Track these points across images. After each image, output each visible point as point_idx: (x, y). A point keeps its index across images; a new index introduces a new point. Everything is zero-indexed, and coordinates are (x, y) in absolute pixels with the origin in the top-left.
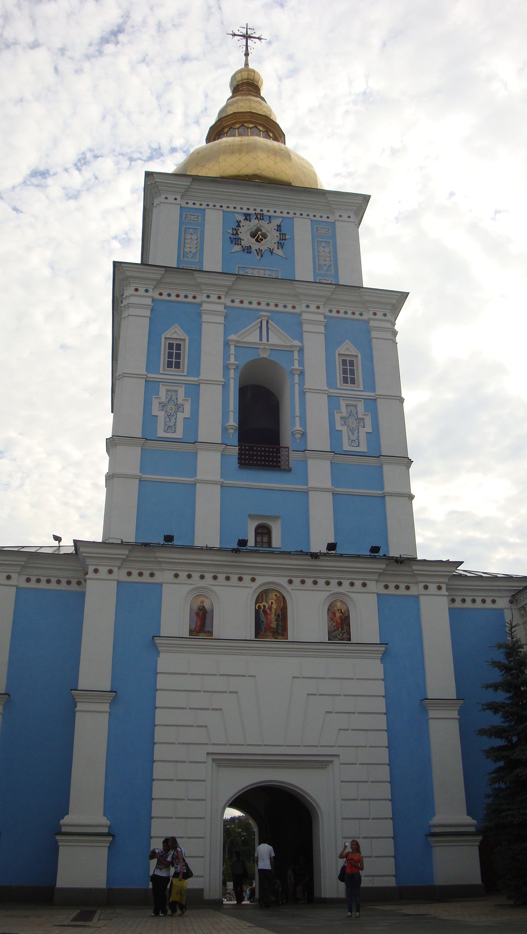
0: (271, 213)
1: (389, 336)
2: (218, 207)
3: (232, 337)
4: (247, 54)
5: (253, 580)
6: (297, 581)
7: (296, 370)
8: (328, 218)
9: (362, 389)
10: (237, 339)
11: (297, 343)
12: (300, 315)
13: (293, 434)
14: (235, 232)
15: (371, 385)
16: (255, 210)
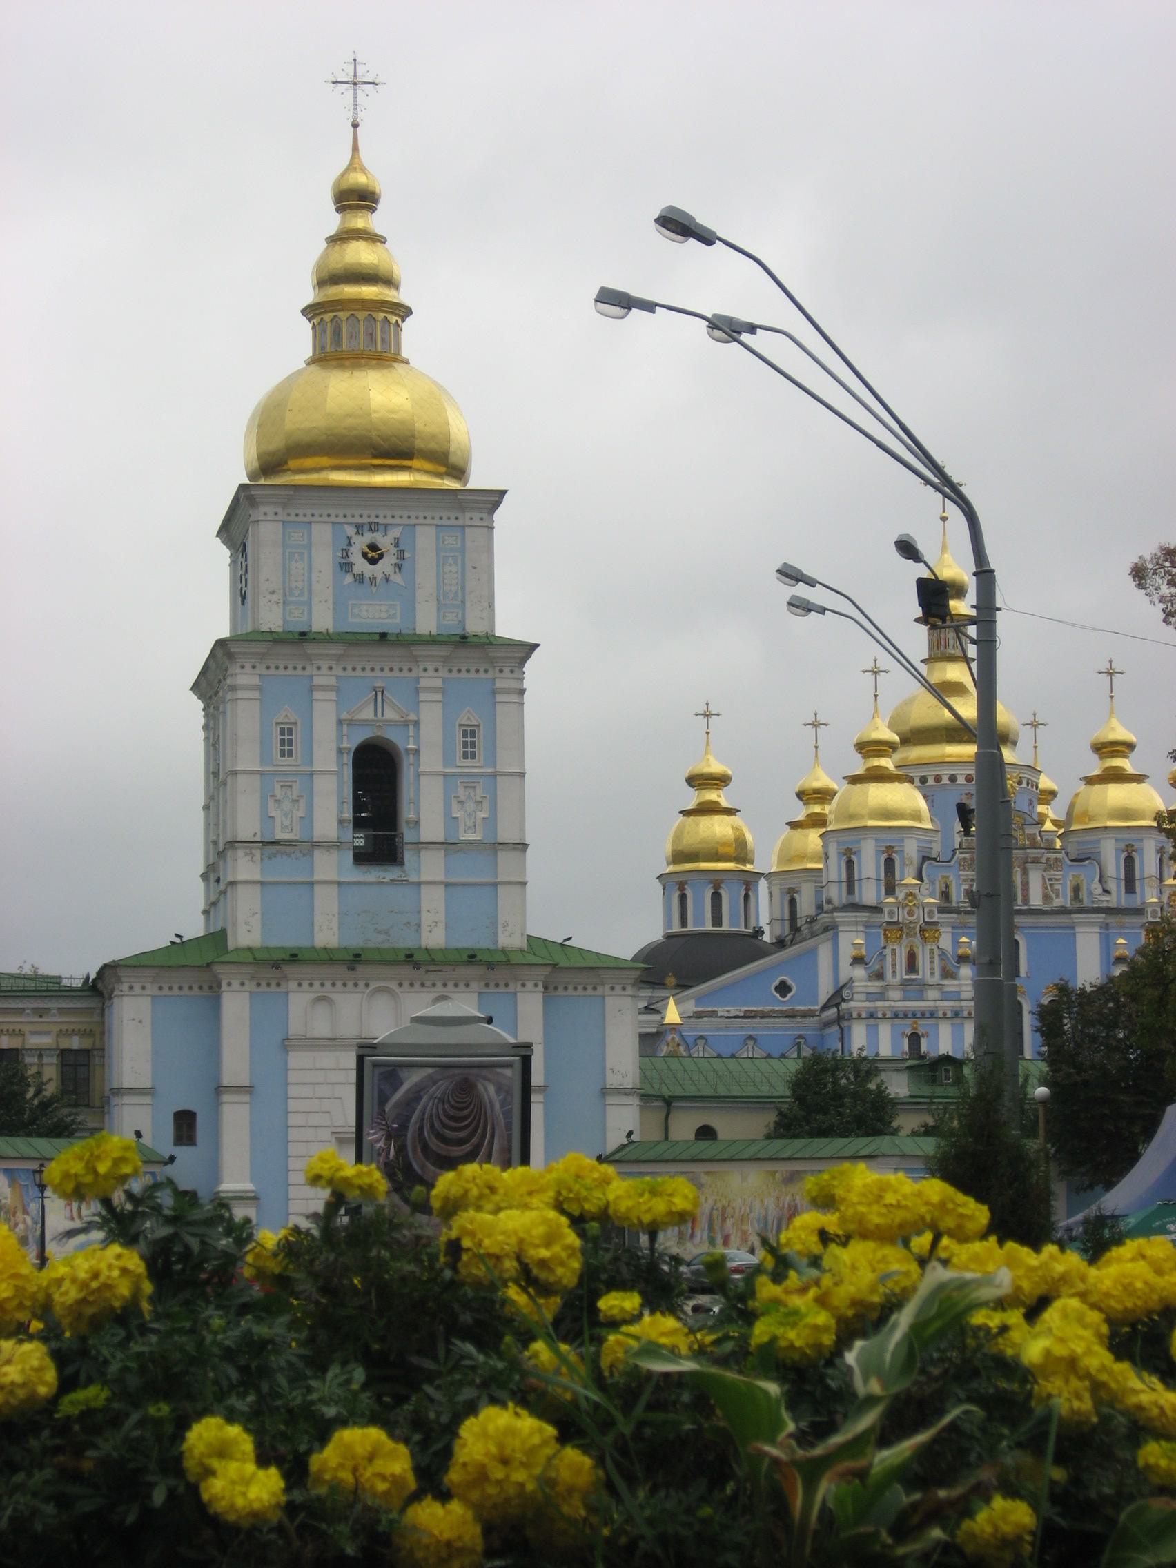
0: (389, 521)
1: (514, 698)
2: (325, 519)
3: (344, 716)
4: (355, 125)
5: (367, 985)
6: (406, 984)
7: (411, 749)
8: (457, 518)
9: (482, 763)
10: (349, 717)
11: (412, 717)
12: (417, 679)
13: (408, 822)
14: (345, 554)
15: (492, 758)
16: (369, 516)
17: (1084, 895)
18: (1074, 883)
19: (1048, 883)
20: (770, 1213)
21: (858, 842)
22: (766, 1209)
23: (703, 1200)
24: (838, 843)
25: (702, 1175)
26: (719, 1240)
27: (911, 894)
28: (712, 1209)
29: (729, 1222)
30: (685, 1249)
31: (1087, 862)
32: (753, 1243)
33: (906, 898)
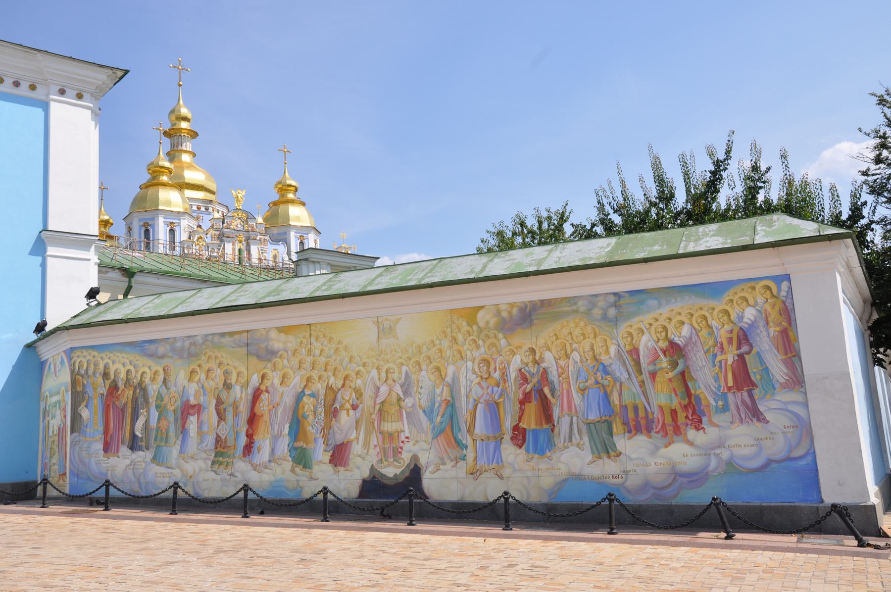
17: (279, 259)
18: (274, 254)
19: (261, 252)
20: (463, 392)
21: (153, 219)
22: (453, 388)
23: (277, 381)
24: (140, 220)
25: (273, 334)
26: (320, 454)
27: (201, 238)
28: (299, 397)
29: (345, 419)
30: (231, 475)
31: (280, 243)
32: (415, 458)
33: (197, 240)
